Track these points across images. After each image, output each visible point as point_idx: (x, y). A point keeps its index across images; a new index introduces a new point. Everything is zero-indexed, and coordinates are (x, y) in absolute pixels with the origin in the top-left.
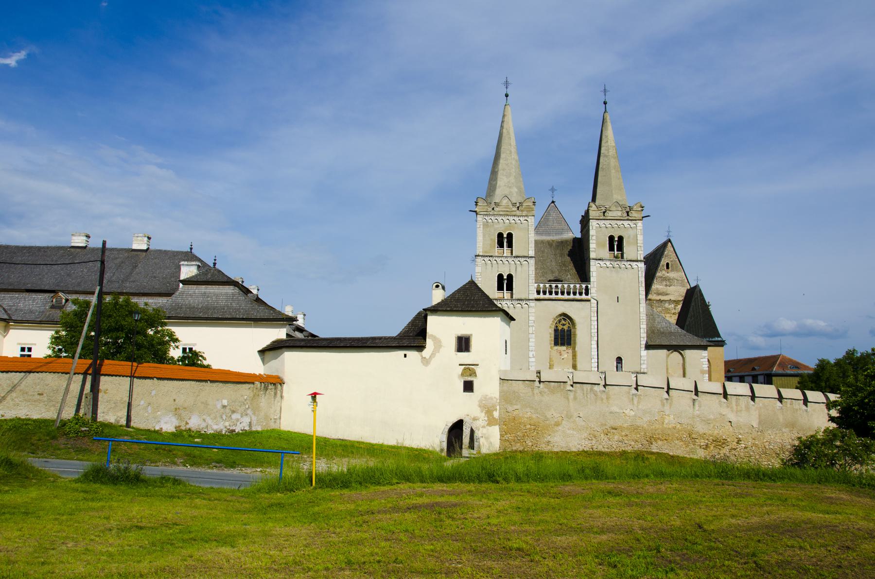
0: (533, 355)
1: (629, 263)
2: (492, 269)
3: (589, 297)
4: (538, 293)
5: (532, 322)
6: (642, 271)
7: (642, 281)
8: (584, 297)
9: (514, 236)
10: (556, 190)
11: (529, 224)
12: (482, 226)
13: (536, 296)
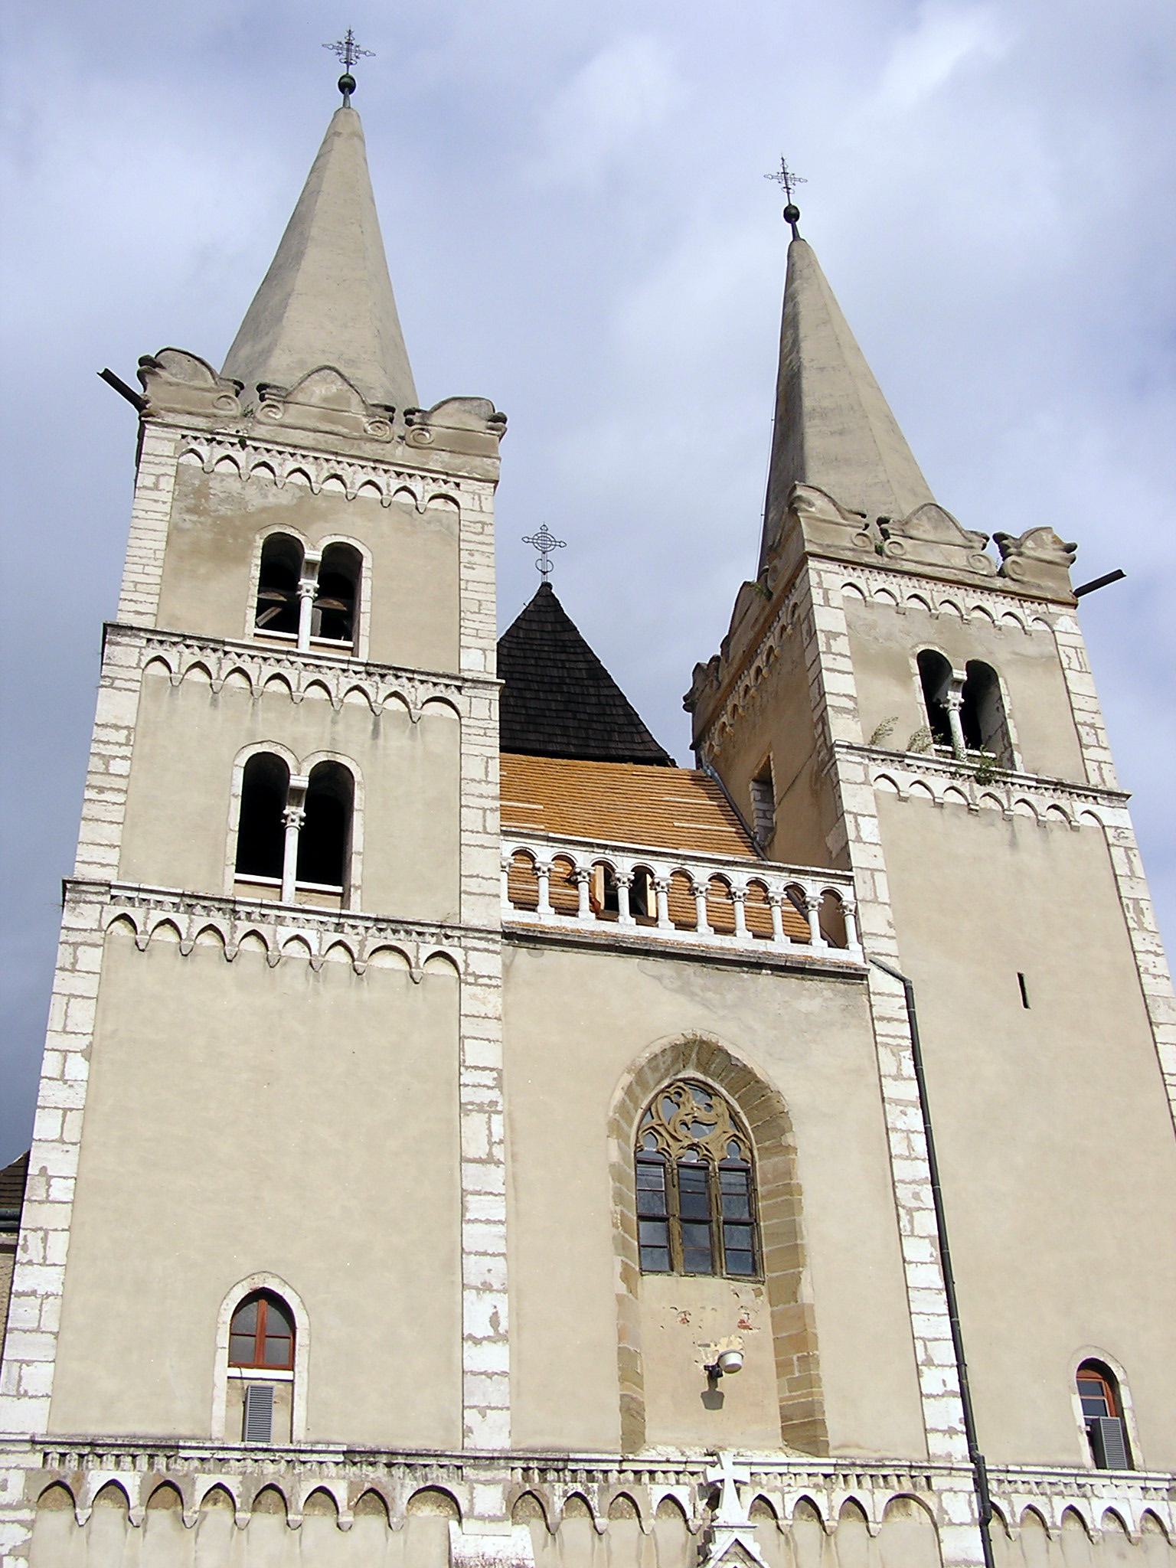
0: (494, 1320)
1: (1049, 798)
3: (852, 955)
5: (488, 1078)
9: (366, 564)
10: (561, 544)
12: (167, 484)
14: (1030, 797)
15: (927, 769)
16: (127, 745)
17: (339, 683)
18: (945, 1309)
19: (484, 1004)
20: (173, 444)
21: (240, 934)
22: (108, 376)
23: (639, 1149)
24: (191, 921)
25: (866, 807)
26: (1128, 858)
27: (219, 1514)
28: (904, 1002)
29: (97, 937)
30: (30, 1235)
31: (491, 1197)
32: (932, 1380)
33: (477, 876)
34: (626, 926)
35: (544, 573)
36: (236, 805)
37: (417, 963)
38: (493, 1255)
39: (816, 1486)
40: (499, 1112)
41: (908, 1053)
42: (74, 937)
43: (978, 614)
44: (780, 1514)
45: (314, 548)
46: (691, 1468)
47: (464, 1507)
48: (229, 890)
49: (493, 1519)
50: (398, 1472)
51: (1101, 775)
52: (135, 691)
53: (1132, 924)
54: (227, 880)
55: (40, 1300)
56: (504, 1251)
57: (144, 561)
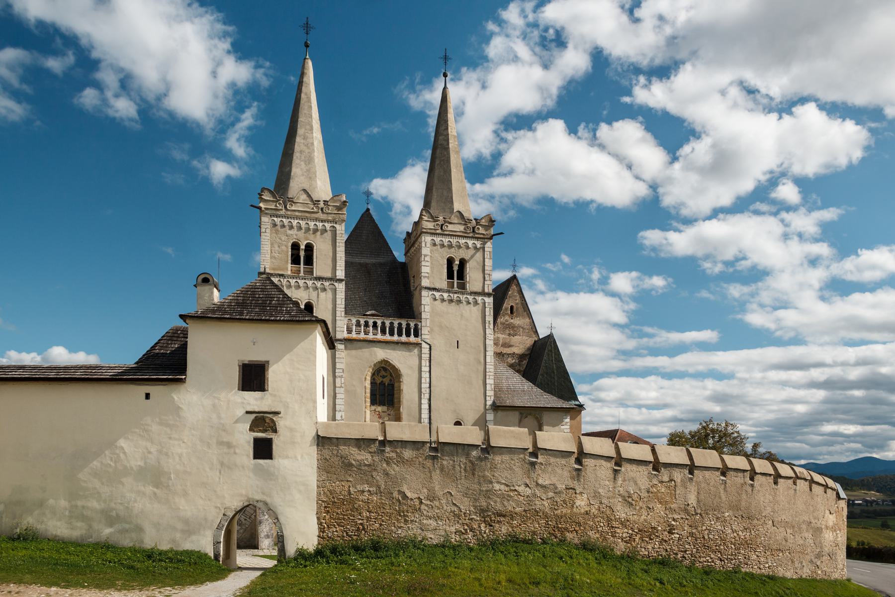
3: (418, 340)
4: (349, 331)
5: (341, 371)
6: (490, 308)
7: (489, 321)
8: (412, 339)
9: (315, 248)
11: (338, 232)
13: (345, 335)
14: (468, 296)
17: (310, 283)
26: (490, 310)
28: (428, 349)
41: (428, 361)
53: (487, 327)
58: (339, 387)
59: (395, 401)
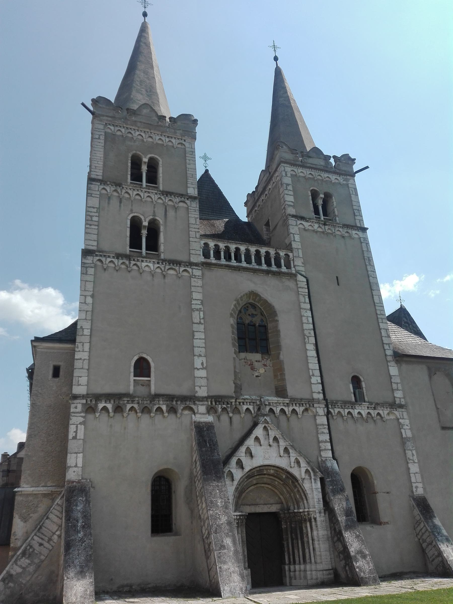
0: (202, 364)
2: (120, 206)
4: (206, 255)
5: (199, 302)
9: (160, 163)
11: (187, 149)
12: (102, 137)
13: (202, 259)
14: (341, 229)
15: (313, 222)
16: (97, 212)
17: (155, 197)
18: (317, 362)
19: (197, 283)
20: (103, 126)
21: (132, 265)
22: (83, 104)
23: (237, 321)
24: (118, 261)
25: (296, 232)
27: (132, 413)
28: (306, 283)
29: (92, 265)
30: (79, 344)
31: (201, 333)
32: (314, 380)
33: (194, 250)
34: (234, 263)
35: (206, 167)
36: (128, 230)
37: (180, 273)
38: (202, 347)
39: (285, 406)
40: (202, 311)
41: (307, 297)
42: (87, 265)
43: (327, 179)
44: (276, 413)
45: (146, 158)
46: (253, 401)
47: (196, 411)
48: (128, 252)
49: (203, 414)
50: (179, 403)
51: (360, 224)
52: (98, 197)
53: (367, 264)
54: (128, 250)
55: (82, 361)
56: (204, 346)
57: (98, 160)
58: (196, 323)
59: (271, 346)
